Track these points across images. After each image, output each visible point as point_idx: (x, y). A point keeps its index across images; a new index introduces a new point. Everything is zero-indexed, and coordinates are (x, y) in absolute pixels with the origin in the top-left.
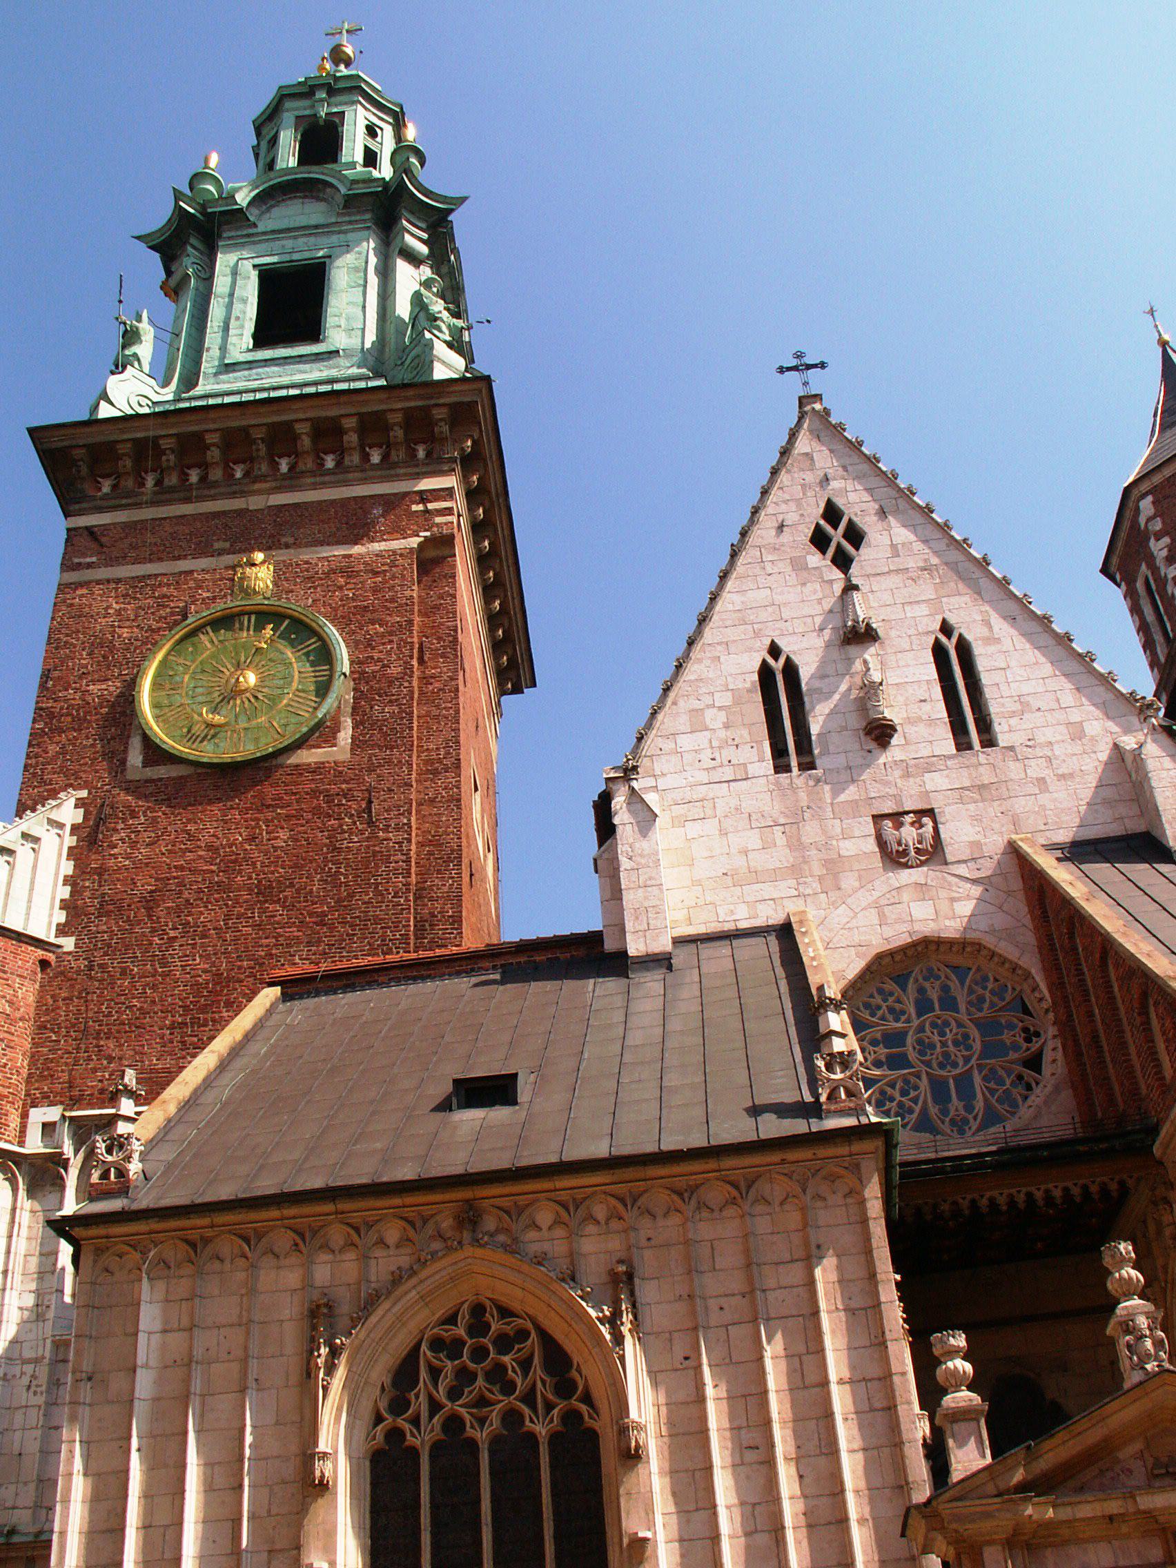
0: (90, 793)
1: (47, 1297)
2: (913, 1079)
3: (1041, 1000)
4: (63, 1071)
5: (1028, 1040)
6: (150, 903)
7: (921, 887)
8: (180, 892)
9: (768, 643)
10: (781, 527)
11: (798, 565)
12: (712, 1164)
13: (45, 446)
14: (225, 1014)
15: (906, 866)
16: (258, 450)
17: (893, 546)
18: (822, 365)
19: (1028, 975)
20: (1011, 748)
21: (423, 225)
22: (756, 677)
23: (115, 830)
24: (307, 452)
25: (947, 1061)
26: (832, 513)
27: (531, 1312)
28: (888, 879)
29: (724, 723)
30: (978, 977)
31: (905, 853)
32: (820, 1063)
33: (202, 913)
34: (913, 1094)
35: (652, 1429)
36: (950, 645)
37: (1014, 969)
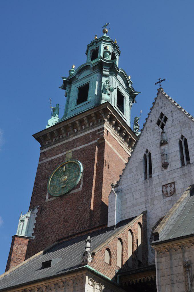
7: (171, 201)
9: (146, 149)
11: (154, 130)
16: (70, 129)
17: (173, 120)
18: (164, 80)
20: (192, 163)
21: (108, 68)
22: (143, 158)
24: (79, 127)
26: (162, 115)
31: (167, 194)
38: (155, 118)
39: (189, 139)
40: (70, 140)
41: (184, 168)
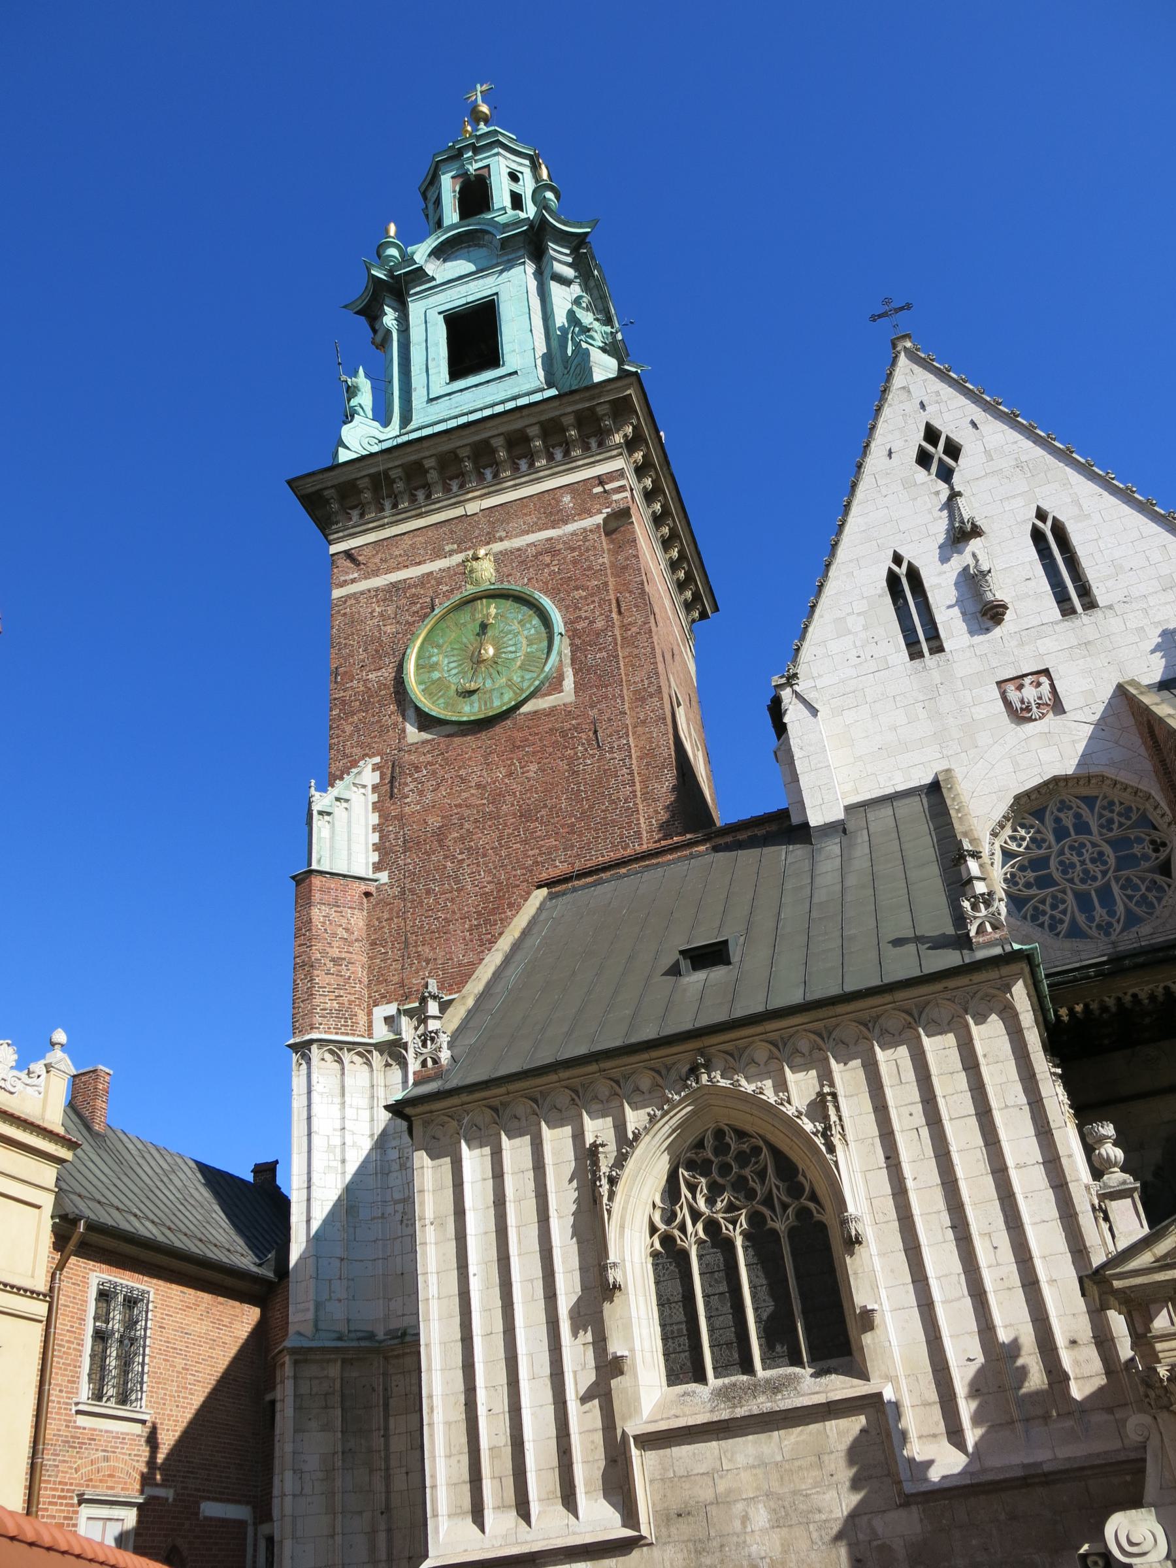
0: (382, 759)
1: (406, 1150)
2: (1060, 895)
3: (1163, 815)
4: (393, 975)
5: (1156, 850)
6: (440, 835)
8: (462, 825)
10: (890, 454)
11: (908, 484)
12: (888, 998)
13: (304, 492)
14: (509, 914)
15: (1030, 720)
18: (908, 307)
19: (1149, 797)
20: (1110, 607)
21: (568, 252)
22: (885, 584)
23: (406, 784)
25: (1087, 877)
26: (931, 435)
27: (761, 1132)
28: (1016, 733)
29: (863, 626)
30: (1105, 803)
31: (1028, 709)
32: (966, 904)
33: (481, 838)
34: (1061, 907)
35: (867, 1219)
36: (1047, 528)
37: (1136, 793)
38: (906, 441)
39: (1072, 521)
40: (472, 508)
41: (1077, 622)
